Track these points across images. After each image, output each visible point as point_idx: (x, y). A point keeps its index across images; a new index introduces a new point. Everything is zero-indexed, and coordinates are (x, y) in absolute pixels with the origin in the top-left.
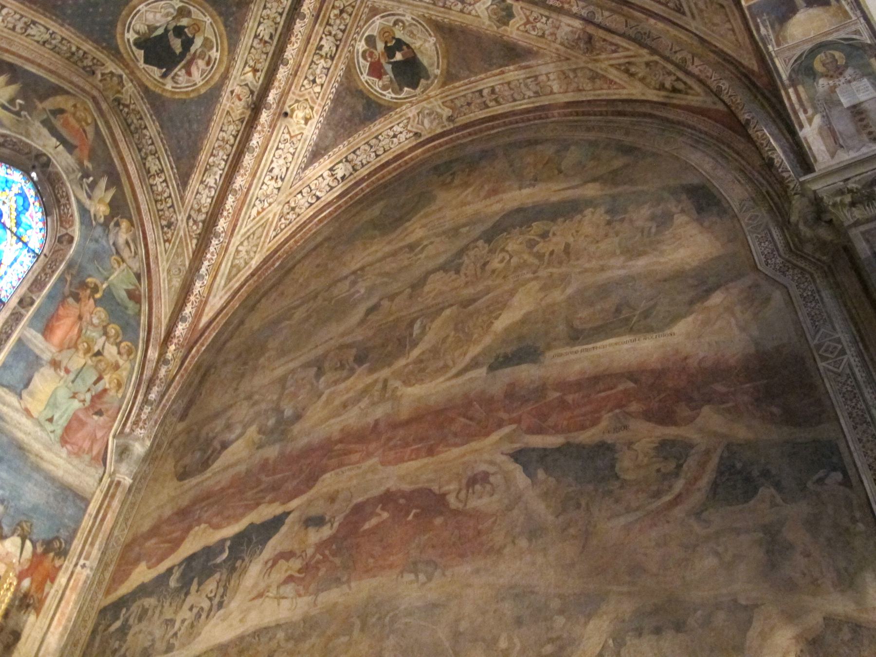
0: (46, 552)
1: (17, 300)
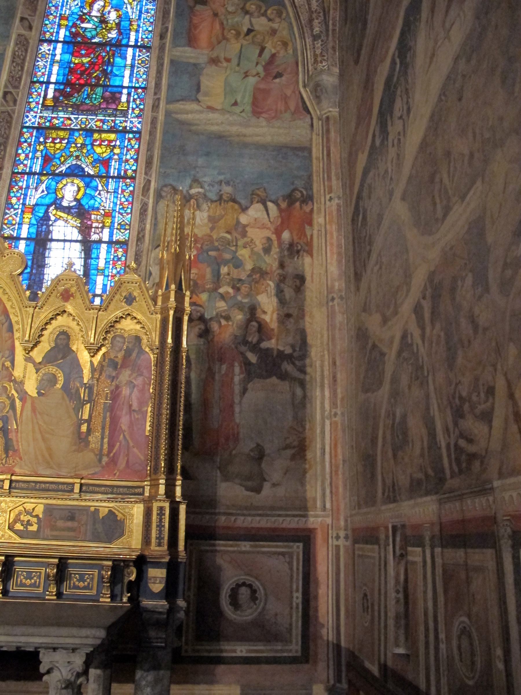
0: (291, 203)
1: (158, 38)
